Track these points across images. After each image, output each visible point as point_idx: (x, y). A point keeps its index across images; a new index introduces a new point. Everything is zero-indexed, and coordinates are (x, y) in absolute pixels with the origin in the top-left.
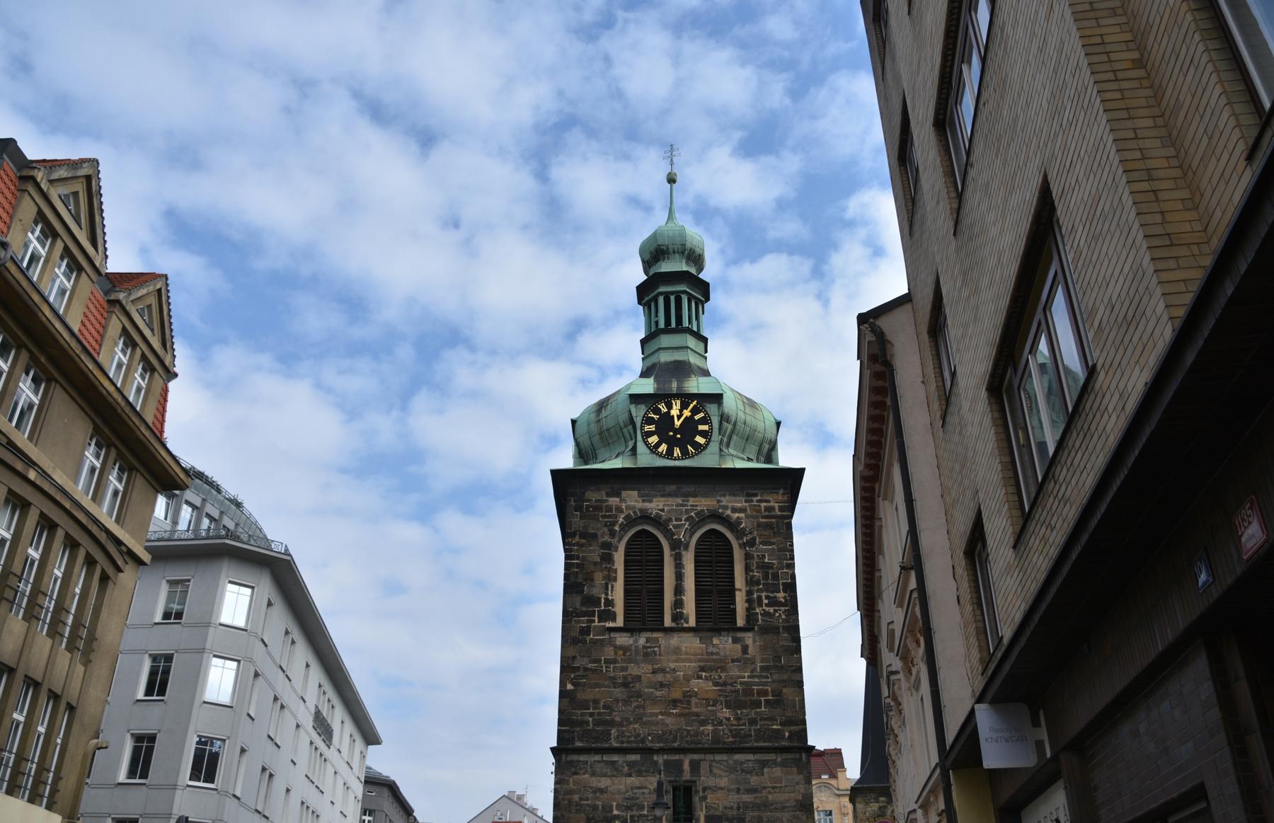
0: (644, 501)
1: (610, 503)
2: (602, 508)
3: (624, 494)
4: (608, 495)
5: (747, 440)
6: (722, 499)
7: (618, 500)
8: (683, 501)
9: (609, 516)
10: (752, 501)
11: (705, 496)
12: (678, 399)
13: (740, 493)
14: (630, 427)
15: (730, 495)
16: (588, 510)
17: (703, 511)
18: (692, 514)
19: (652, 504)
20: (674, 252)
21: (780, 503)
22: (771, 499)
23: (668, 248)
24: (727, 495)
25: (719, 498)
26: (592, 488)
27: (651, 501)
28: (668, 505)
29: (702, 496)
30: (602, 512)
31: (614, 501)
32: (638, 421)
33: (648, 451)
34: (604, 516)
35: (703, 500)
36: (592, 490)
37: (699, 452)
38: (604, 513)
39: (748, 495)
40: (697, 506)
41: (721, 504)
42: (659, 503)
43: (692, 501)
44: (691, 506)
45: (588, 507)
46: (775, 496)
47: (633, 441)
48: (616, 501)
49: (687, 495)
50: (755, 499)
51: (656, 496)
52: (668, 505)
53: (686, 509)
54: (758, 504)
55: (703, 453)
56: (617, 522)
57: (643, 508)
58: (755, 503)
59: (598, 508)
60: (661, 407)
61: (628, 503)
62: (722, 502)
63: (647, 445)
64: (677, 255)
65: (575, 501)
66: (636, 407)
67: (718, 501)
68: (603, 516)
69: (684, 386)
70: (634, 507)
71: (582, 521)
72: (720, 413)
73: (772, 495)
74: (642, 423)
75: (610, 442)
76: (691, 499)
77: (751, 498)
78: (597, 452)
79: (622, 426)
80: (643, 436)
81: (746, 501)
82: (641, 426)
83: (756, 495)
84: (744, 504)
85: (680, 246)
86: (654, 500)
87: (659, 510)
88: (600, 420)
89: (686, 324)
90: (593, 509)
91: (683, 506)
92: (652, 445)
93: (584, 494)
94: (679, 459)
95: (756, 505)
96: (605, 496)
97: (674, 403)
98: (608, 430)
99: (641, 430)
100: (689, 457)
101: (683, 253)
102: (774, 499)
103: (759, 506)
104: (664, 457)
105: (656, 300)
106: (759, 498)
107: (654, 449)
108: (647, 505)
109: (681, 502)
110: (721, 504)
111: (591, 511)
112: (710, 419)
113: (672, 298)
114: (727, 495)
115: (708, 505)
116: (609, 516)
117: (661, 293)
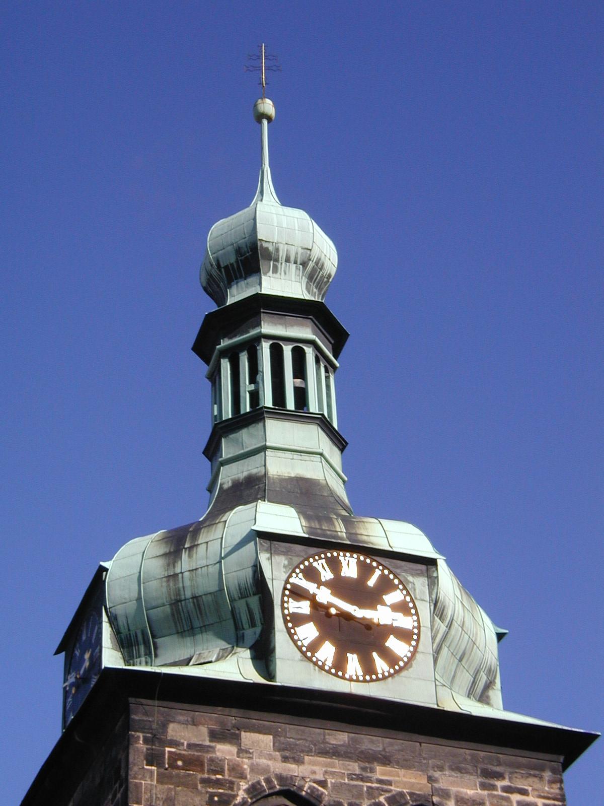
0: (285, 759)
1: (219, 754)
2: (202, 764)
3: (247, 737)
4: (214, 736)
5: (460, 660)
6: (437, 774)
7: (234, 749)
8: (364, 769)
9: (218, 783)
10: (494, 787)
11: (406, 765)
12: (352, 556)
13: (469, 767)
14: (254, 601)
15: (452, 769)
16: (173, 766)
17: (401, 794)
18: (382, 799)
19: (301, 768)
20: (288, 260)
21: (548, 798)
22: (530, 789)
23: (277, 250)
24: (446, 768)
25: (431, 773)
26: (181, 718)
27: (299, 761)
28: (333, 774)
29: (398, 763)
30: (202, 771)
31: (225, 751)
32: (276, 588)
33: (299, 655)
34: (206, 782)
35: (402, 772)
36: (179, 722)
37: (396, 672)
38: (206, 776)
39: (488, 774)
40: (389, 783)
41: (436, 785)
42: (316, 768)
43: (380, 772)
44: (380, 781)
45: (174, 757)
46: (538, 785)
47: (258, 629)
48: (230, 753)
49: (369, 758)
50: (500, 784)
51: (309, 752)
52: (333, 774)
53: (369, 788)
54: (505, 794)
55: (404, 673)
56: (235, 796)
57: (284, 774)
58: (500, 793)
59: (193, 763)
60: (320, 568)
61: (256, 760)
62: (436, 781)
63: (295, 642)
64: (293, 266)
65: (146, 741)
66: (270, 559)
67: (430, 779)
68: (206, 782)
69: (359, 532)
70: (266, 770)
71: (160, 787)
72: (434, 597)
73: (531, 780)
74: (284, 595)
75: (197, 624)
76: (379, 768)
77: (492, 782)
78: (159, 641)
79: (236, 595)
80: (286, 622)
81: (484, 786)
82: (283, 602)
83: (500, 776)
84: (479, 791)
85: (300, 251)
86: (306, 758)
87: (315, 782)
88: (175, 576)
89: (313, 407)
90: (184, 762)
91: (362, 779)
92: (306, 643)
93: (164, 726)
94: (357, 681)
95: (503, 798)
96: (208, 739)
97: (344, 563)
98: (195, 598)
99: (283, 608)
100: (378, 679)
101: (304, 264)
102: (533, 790)
103: (508, 799)
104: (329, 672)
105: (252, 347)
106: (506, 783)
107: (308, 652)
108: (293, 769)
109: (358, 772)
110: (436, 785)
111: (178, 768)
112: (415, 607)
113: (287, 351)
114: (446, 768)
115: (412, 785)
116: (218, 783)
117: (268, 337)
